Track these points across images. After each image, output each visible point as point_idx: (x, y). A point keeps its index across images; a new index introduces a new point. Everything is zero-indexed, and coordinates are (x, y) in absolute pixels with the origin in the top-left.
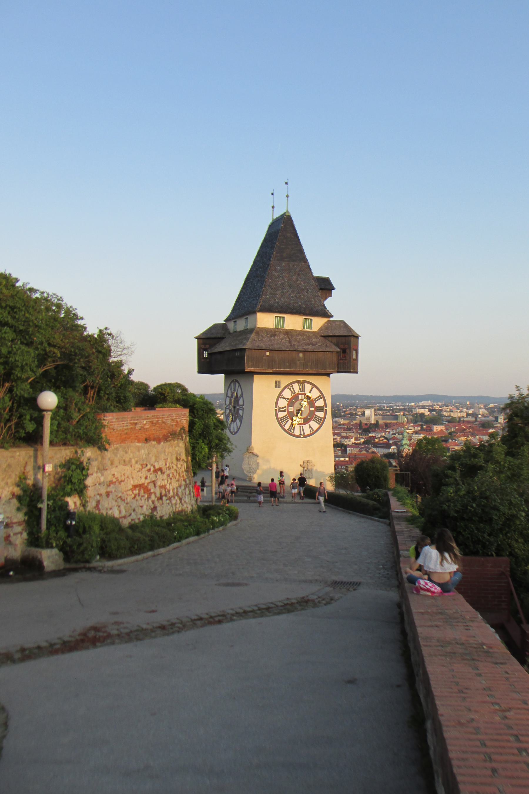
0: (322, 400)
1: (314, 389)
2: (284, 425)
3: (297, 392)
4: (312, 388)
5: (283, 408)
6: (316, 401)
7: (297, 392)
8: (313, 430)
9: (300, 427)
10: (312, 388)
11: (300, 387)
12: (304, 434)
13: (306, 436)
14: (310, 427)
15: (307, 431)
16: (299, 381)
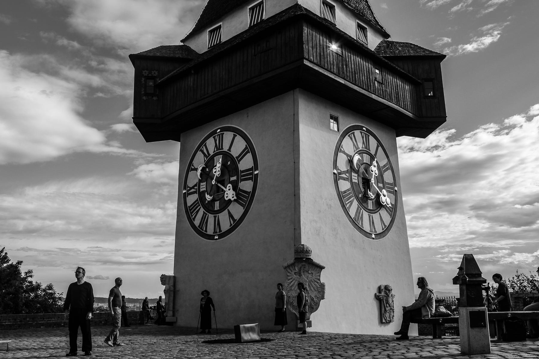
0: (249, 156)
1: (238, 138)
2: (194, 219)
3: (212, 153)
4: (235, 136)
5: (193, 188)
6: (239, 161)
7: (212, 153)
8: (234, 220)
9: (215, 217)
10: (235, 136)
11: (215, 141)
12: (220, 231)
13: (222, 236)
14: (231, 216)
15: (225, 225)
16: (215, 132)
